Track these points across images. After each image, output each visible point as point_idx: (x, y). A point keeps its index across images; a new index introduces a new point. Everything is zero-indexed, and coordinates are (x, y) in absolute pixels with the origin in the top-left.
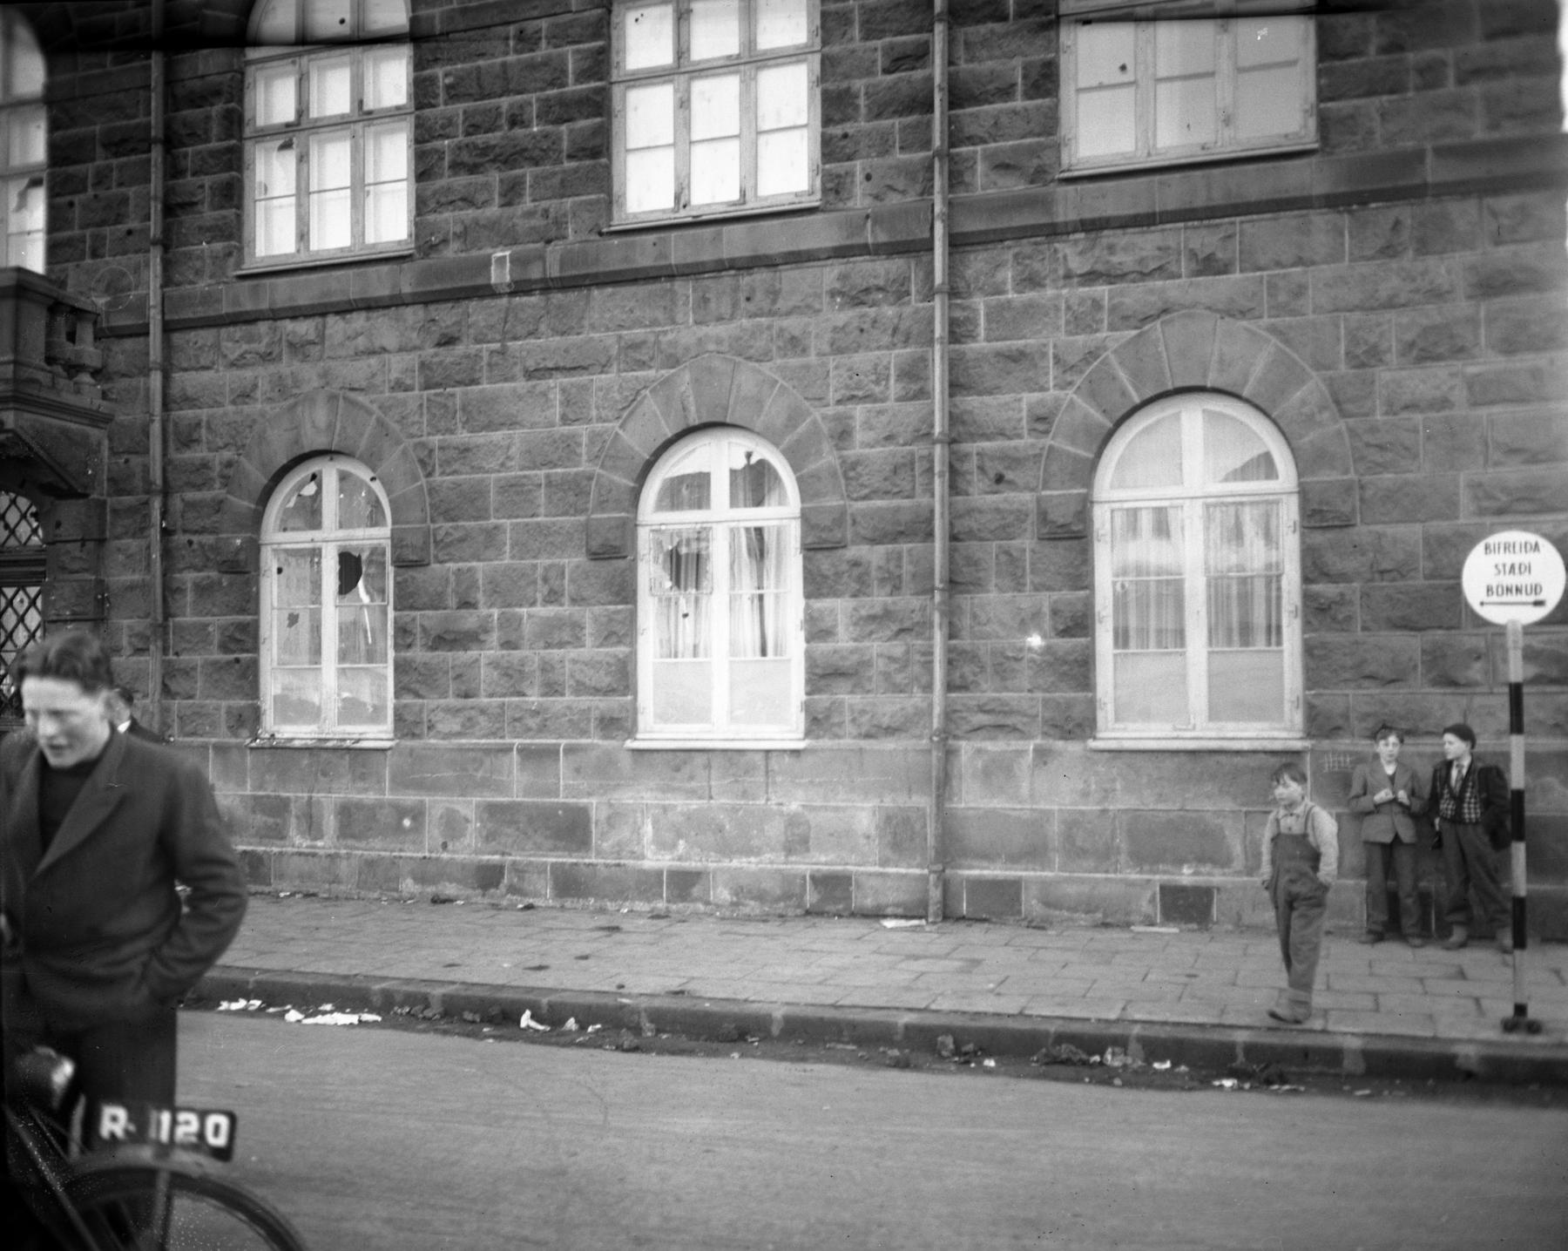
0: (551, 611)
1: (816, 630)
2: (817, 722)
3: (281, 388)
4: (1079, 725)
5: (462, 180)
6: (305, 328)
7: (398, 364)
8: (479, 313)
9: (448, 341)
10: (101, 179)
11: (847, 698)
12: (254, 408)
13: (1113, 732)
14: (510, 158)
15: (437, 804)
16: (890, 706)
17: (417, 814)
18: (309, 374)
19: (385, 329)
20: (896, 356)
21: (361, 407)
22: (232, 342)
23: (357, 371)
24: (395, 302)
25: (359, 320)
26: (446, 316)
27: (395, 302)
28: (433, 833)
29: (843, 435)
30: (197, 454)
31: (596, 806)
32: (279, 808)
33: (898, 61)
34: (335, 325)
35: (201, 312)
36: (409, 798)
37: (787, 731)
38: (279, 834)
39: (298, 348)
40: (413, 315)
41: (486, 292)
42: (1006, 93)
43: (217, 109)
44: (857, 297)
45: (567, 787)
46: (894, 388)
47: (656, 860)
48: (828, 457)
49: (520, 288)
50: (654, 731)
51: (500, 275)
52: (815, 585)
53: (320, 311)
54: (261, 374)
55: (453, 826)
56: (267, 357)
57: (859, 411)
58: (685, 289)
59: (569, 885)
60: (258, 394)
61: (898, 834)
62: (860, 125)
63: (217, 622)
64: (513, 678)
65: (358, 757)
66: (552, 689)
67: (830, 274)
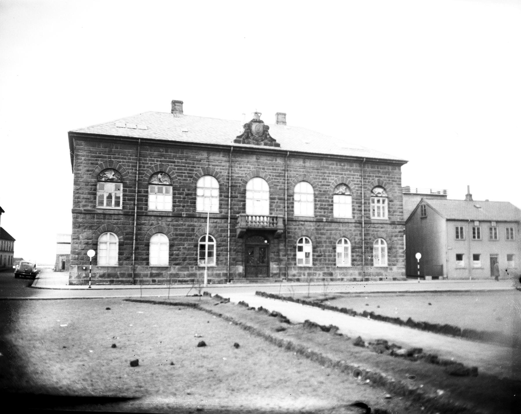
1: (352, 256)
2: (353, 264)
3: (300, 229)
4: (372, 265)
5: (319, 210)
6: (303, 223)
7: (313, 228)
8: (321, 224)
9: (318, 226)
10: (277, 202)
11: (355, 263)
12: (296, 230)
13: (375, 265)
14: (324, 209)
15: (318, 272)
16: (359, 263)
17: (316, 273)
18: (303, 227)
19: (312, 224)
20: (359, 232)
22: (294, 223)
23: (309, 228)
24: (313, 221)
25: (308, 223)
26: (318, 224)
27: (313, 221)
28: (317, 275)
29: (355, 239)
30: (290, 235)
31: (333, 272)
32: (301, 273)
33: (359, 207)
34: (306, 223)
36: (315, 272)
37: (349, 264)
38: (300, 276)
39: (302, 225)
40: (314, 223)
41: (322, 222)
43: (292, 198)
44: (356, 227)
45: (331, 270)
47: (339, 277)
48: (353, 241)
49: (326, 222)
50: (338, 265)
51: (324, 220)
52: (352, 252)
53: (304, 221)
54: (297, 227)
55: (319, 274)
56: (298, 225)
57: (356, 237)
58: (341, 224)
59: (332, 280)
61: (360, 274)
63: (293, 253)
64: (325, 260)
65: (309, 268)
66: (329, 261)
67: (354, 225)
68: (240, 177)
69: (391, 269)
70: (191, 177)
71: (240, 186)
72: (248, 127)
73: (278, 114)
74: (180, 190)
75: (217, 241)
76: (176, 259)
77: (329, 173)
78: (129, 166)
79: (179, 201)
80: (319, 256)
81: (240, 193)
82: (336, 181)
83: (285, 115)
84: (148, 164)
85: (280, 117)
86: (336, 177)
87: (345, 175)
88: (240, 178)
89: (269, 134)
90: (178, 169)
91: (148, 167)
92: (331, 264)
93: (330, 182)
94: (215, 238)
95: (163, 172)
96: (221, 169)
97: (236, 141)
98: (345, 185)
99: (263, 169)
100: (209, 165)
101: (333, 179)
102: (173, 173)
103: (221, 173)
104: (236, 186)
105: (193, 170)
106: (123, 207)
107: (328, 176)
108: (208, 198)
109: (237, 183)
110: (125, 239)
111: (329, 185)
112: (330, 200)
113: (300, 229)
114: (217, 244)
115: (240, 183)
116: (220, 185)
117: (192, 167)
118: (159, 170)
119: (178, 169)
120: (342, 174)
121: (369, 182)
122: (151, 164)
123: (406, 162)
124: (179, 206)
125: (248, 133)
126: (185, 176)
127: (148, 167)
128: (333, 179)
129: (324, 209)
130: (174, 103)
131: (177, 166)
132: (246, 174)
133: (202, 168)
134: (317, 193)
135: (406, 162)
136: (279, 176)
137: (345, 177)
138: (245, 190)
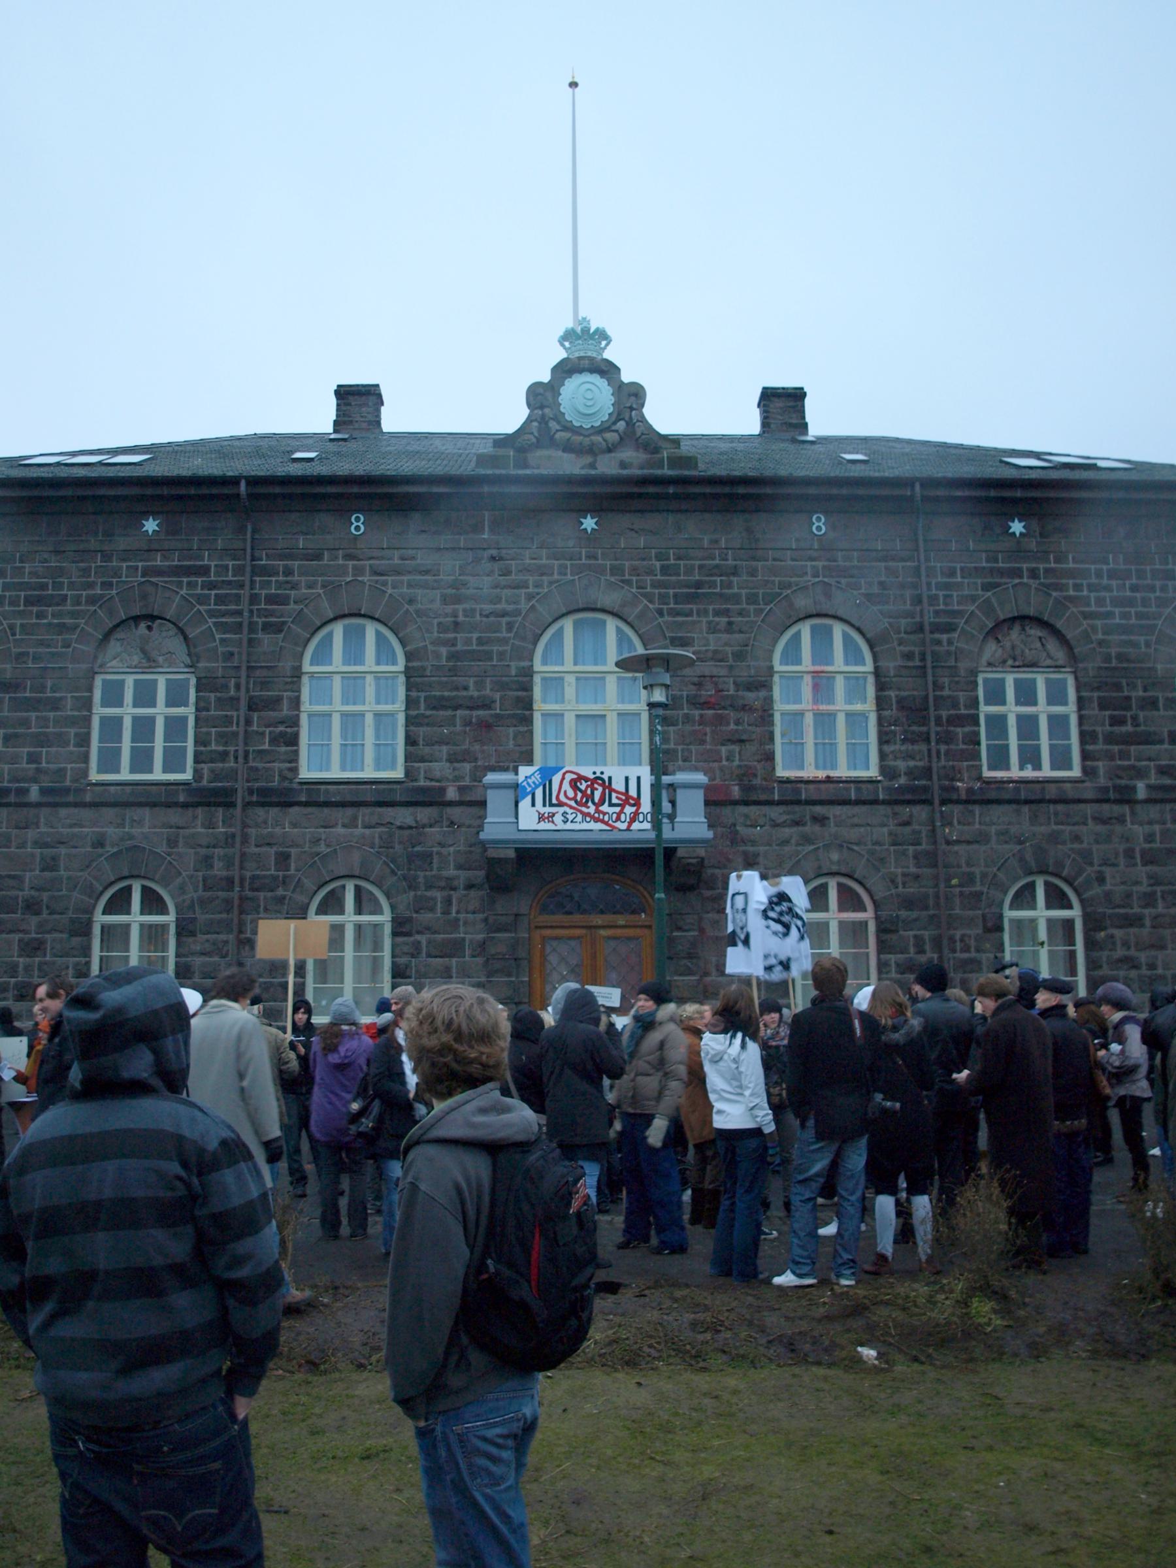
0: (966, 955)
9: (907, 823)
21: (852, 850)
29: (1101, 879)
34: (837, 810)
35: (763, 797)
42: (1161, 742)
43: (763, 694)
46: (1122, 860)
60: (793, 841)
62: (1100, 746)
67: (1089, 809)
68: (504, 614)
70: (278, 628)
71: (501, 655)
72: (541, 397)
74: (226, 687)
77: (952, 573)
79: (224, 738)
81: (502, 686)
82: (987, 608)
84: (91, 585)
86: (986, 587)
87: (1034, 574)
88: (504, 620)
89: (643, 419)
90: (220, 600)
91: (92, 600)
93: (959, 613)
94: (388, 896)
95: (152, 618)
96: (410, 586)
97: (482, 460)
99: (615, 570)
100: (358, 571)
101: (973, 599)
103: (411, 601)
104: (488, 656)
105: (282, 600)
108: (351, 713)
109: (489, 641)
112: (962, 696)
113: (807, 839)
114: (394, 920)
115: (505, 641)
116: (409, 656)
117: (280, 585)
118: (136, 611)
119: (220, 600)
120: (1018, 573)
122: (107, 585)
124: (224, 756)
127: (92, 600)
128: (973, 599)
131: (212, 586)
132: (530, 597)
133: (323, 586)
134: (890, 665)
137: (1033, 583)
138: (529, 673)
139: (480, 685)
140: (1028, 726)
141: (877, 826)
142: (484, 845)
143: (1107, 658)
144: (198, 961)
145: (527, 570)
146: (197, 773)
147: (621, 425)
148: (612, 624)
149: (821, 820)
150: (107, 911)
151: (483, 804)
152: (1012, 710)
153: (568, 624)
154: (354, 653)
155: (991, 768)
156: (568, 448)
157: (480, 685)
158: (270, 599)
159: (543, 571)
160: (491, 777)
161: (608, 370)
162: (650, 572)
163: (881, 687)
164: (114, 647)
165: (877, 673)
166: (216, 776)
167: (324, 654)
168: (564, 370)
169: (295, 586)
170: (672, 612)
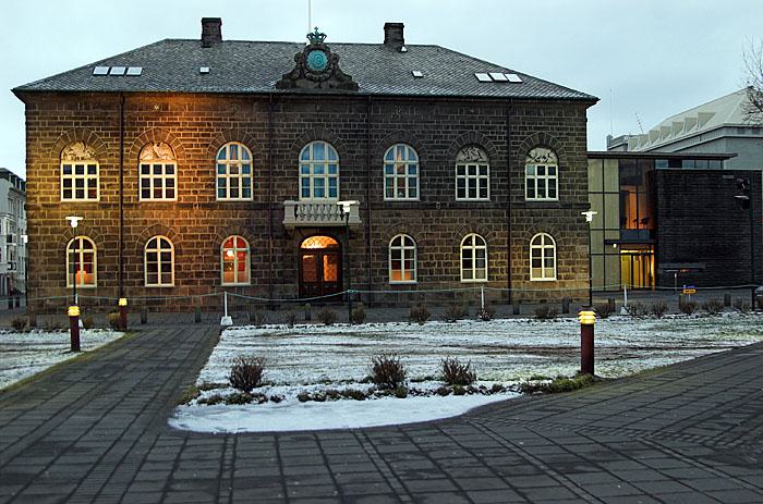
29: (494, 235)
69: (563, 285)
72: (301, 59)
73: (388, 26)
75: (251, 245)
76: (186, 275)
77: (448, 127)
78: (107, 135)
80: (428, 264)
82: (460, 140)
83: (401, 26)
85: (391, 31)
86: (460, 133)
87: (477, 128)
92: (451, 279)
98: (478, 145)
99: (329, 126)
100: (235, 125)
102: (177, 142)
106: (255, 198)
107: (446, 132)
110: (106, 246)
111: (445, 147)
117: (207, 130)
121: (522, 138)
123: (594, 101)
125: (302, 69)
126: (197, 146)
129: (438, 186)
130: (205, 22)
131: (181, 130)
135: (594, 101)
136: (356, 136)
139: (280, 167)
140: (472, 182)
141: (418, 216)
142: (283, 225)
143: (501, 158)
144: (183, 264)
145: (296, 125)
146: (179, 199)
147: (330, 71)
148: (326, 145)
149: (398, 215)
150: (148, 247)
151: (284, 209)
152: (467, 177)
153: (311, 145)
154: (234, 156)
155: (459, 197)
156: (311, 79)
157: (280, 167)
158: (203, 135)
159: (303, 125)
160: (286, 202)
161: (325, 48)
162: (341, 126)
163: (421, 168)
164: (146, 153)
165: (420, 163)
166: (186, 199)
167: (223, 156)
168: (309, 49)
169: (212, 130)
170: (348, 141)
